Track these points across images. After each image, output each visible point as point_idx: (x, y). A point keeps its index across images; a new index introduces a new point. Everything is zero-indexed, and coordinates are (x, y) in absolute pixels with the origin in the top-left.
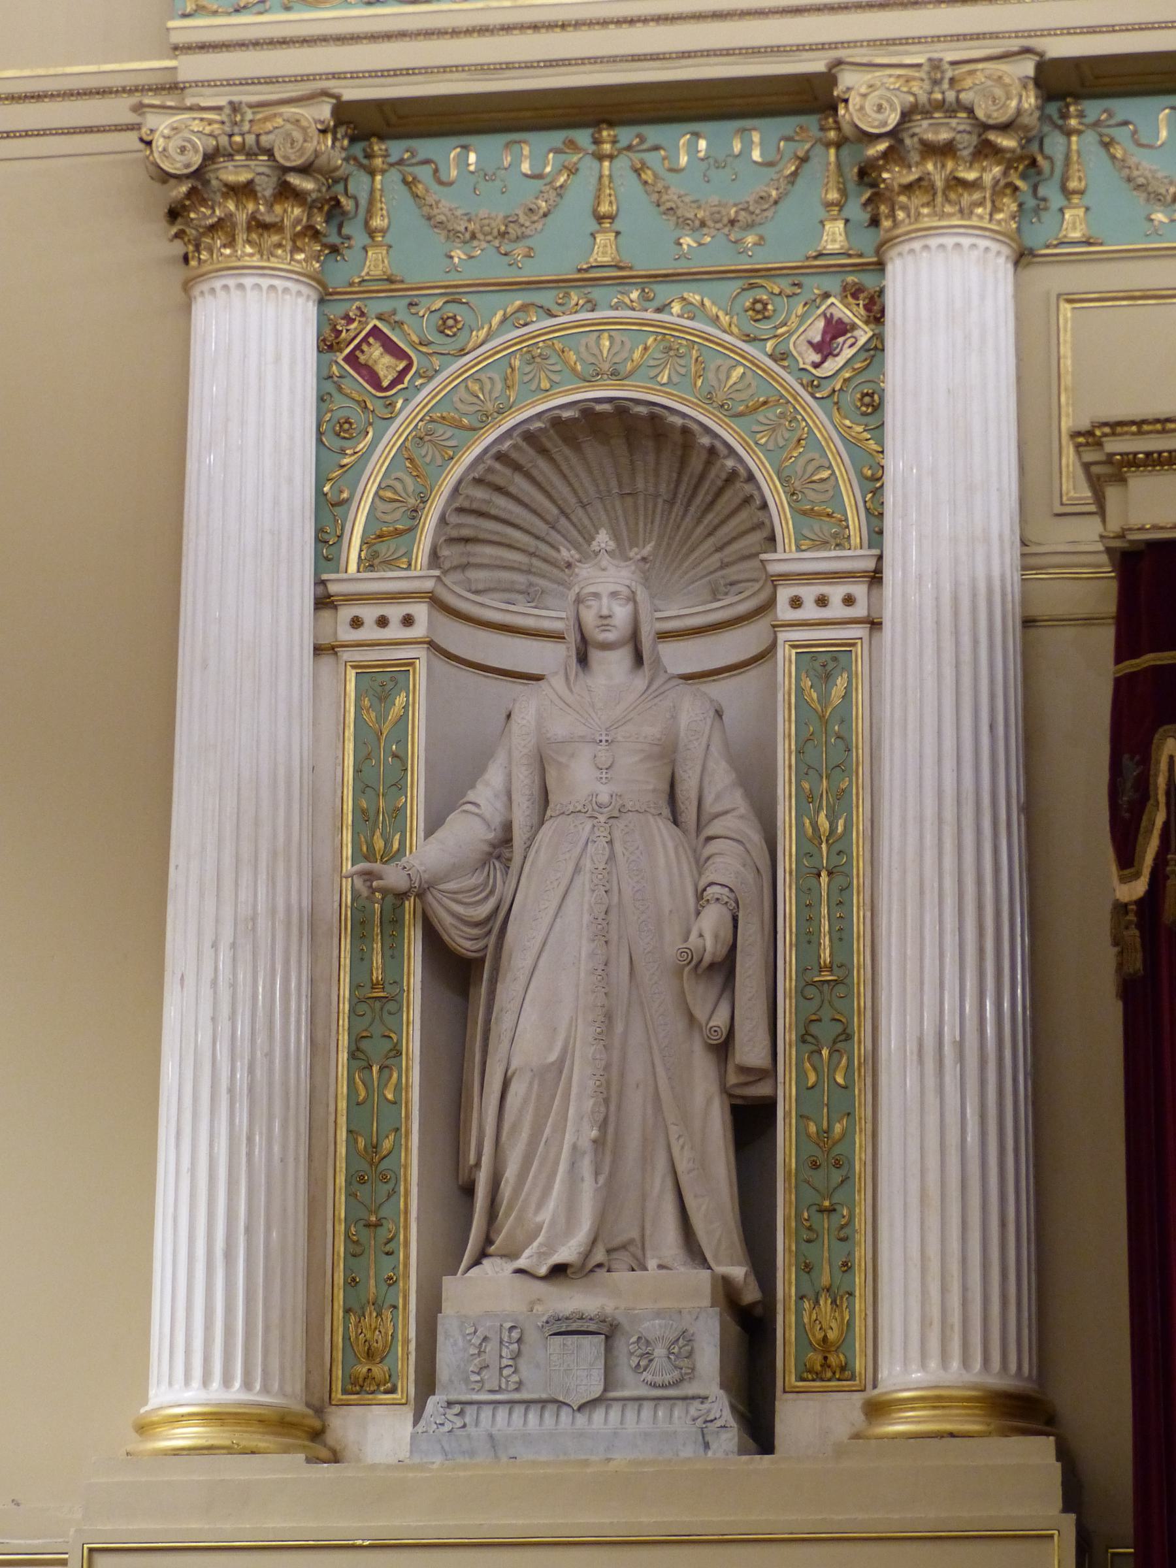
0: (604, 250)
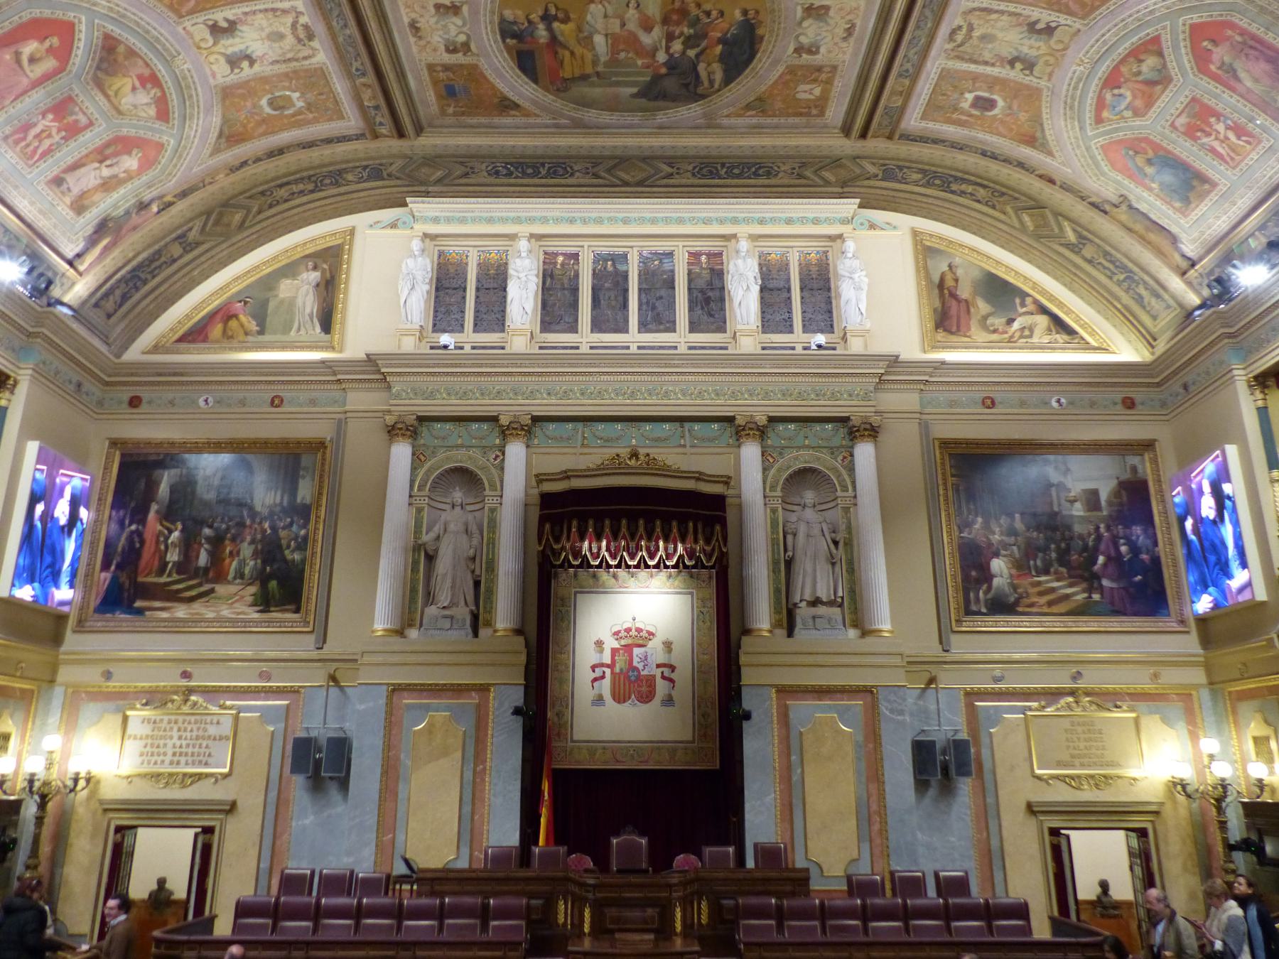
0: (460, 441)
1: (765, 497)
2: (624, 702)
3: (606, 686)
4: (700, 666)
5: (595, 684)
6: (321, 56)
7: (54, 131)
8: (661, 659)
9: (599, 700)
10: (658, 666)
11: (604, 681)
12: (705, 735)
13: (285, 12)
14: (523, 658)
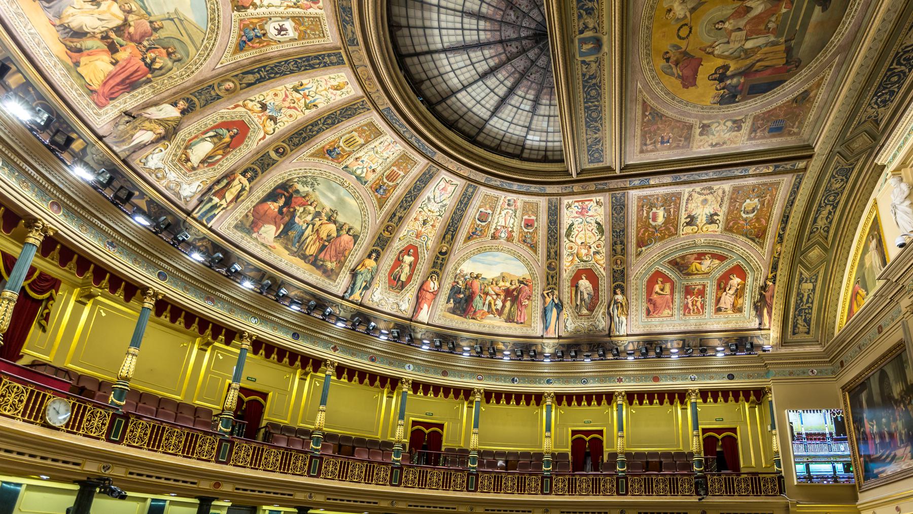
6: (727, 186)
7: (696, 299)
13: (690, 196)
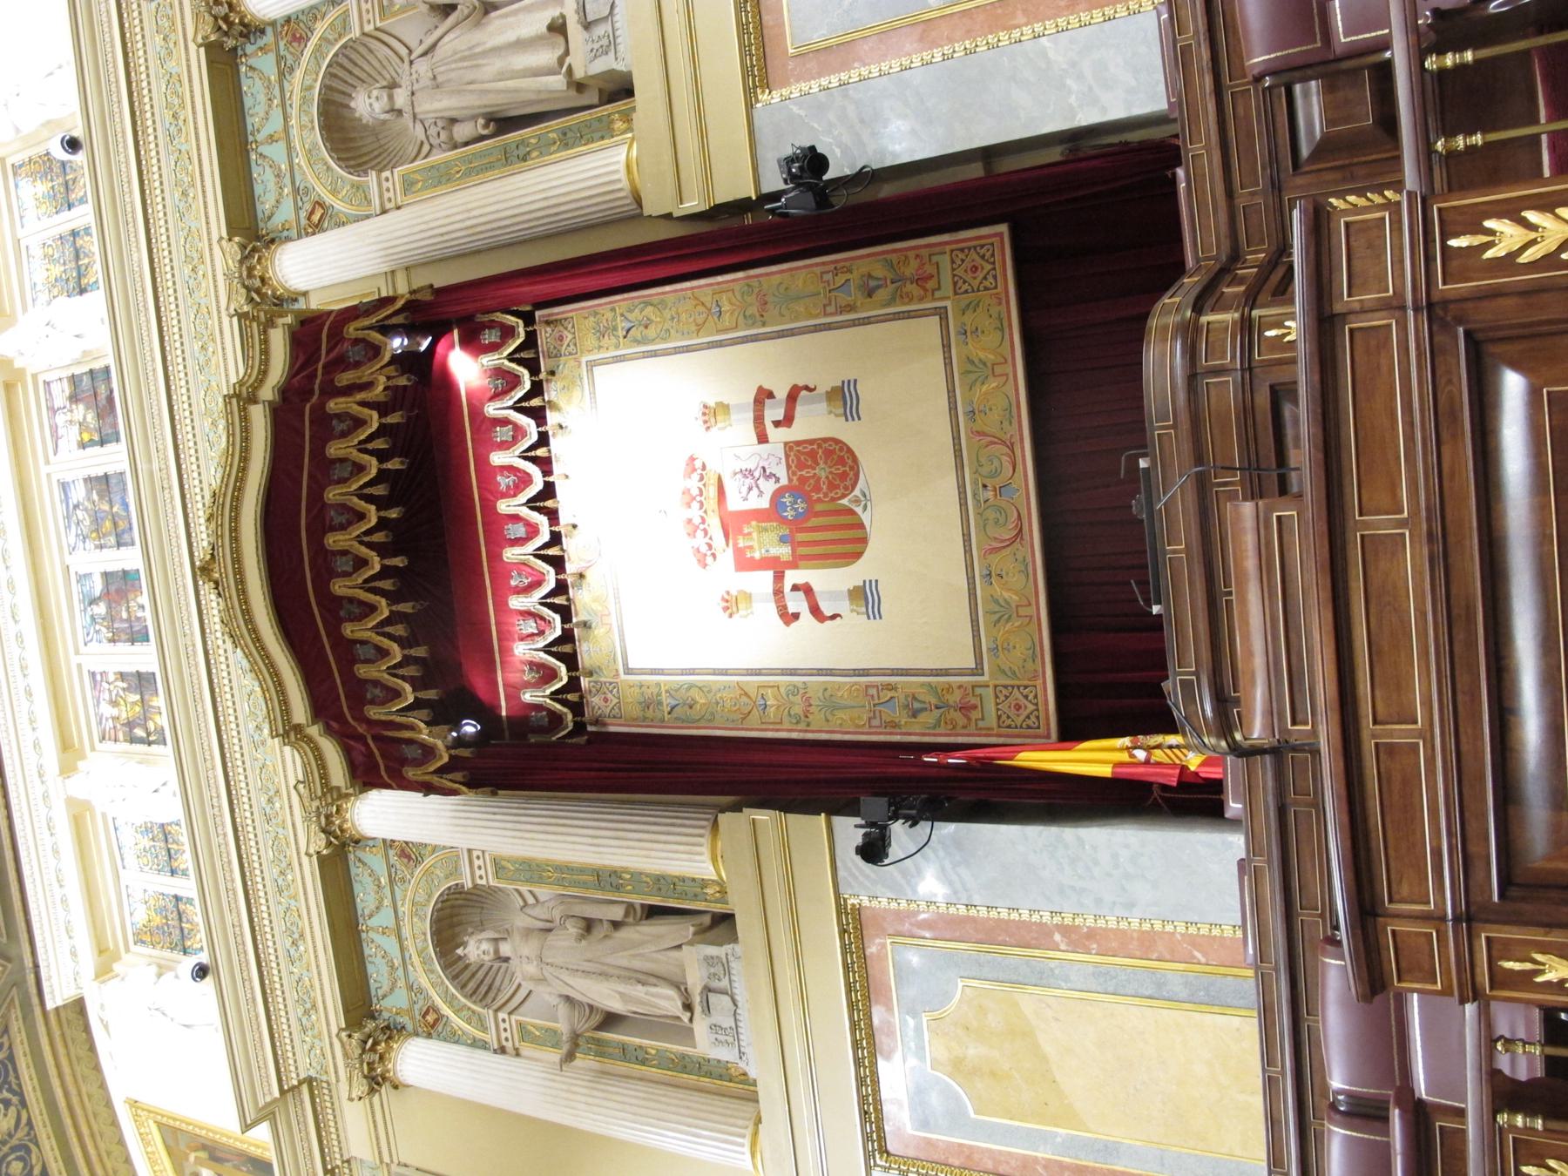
1: (384, 212)
2: (861, 526)
3: (829, 581)
4: (751, 321)
5: (828, 613)
8: (742, 428)
9: (864, 596)
10: (763, 438)
11: (816, 588)
12: (921, 280)
14: (763, 816)
